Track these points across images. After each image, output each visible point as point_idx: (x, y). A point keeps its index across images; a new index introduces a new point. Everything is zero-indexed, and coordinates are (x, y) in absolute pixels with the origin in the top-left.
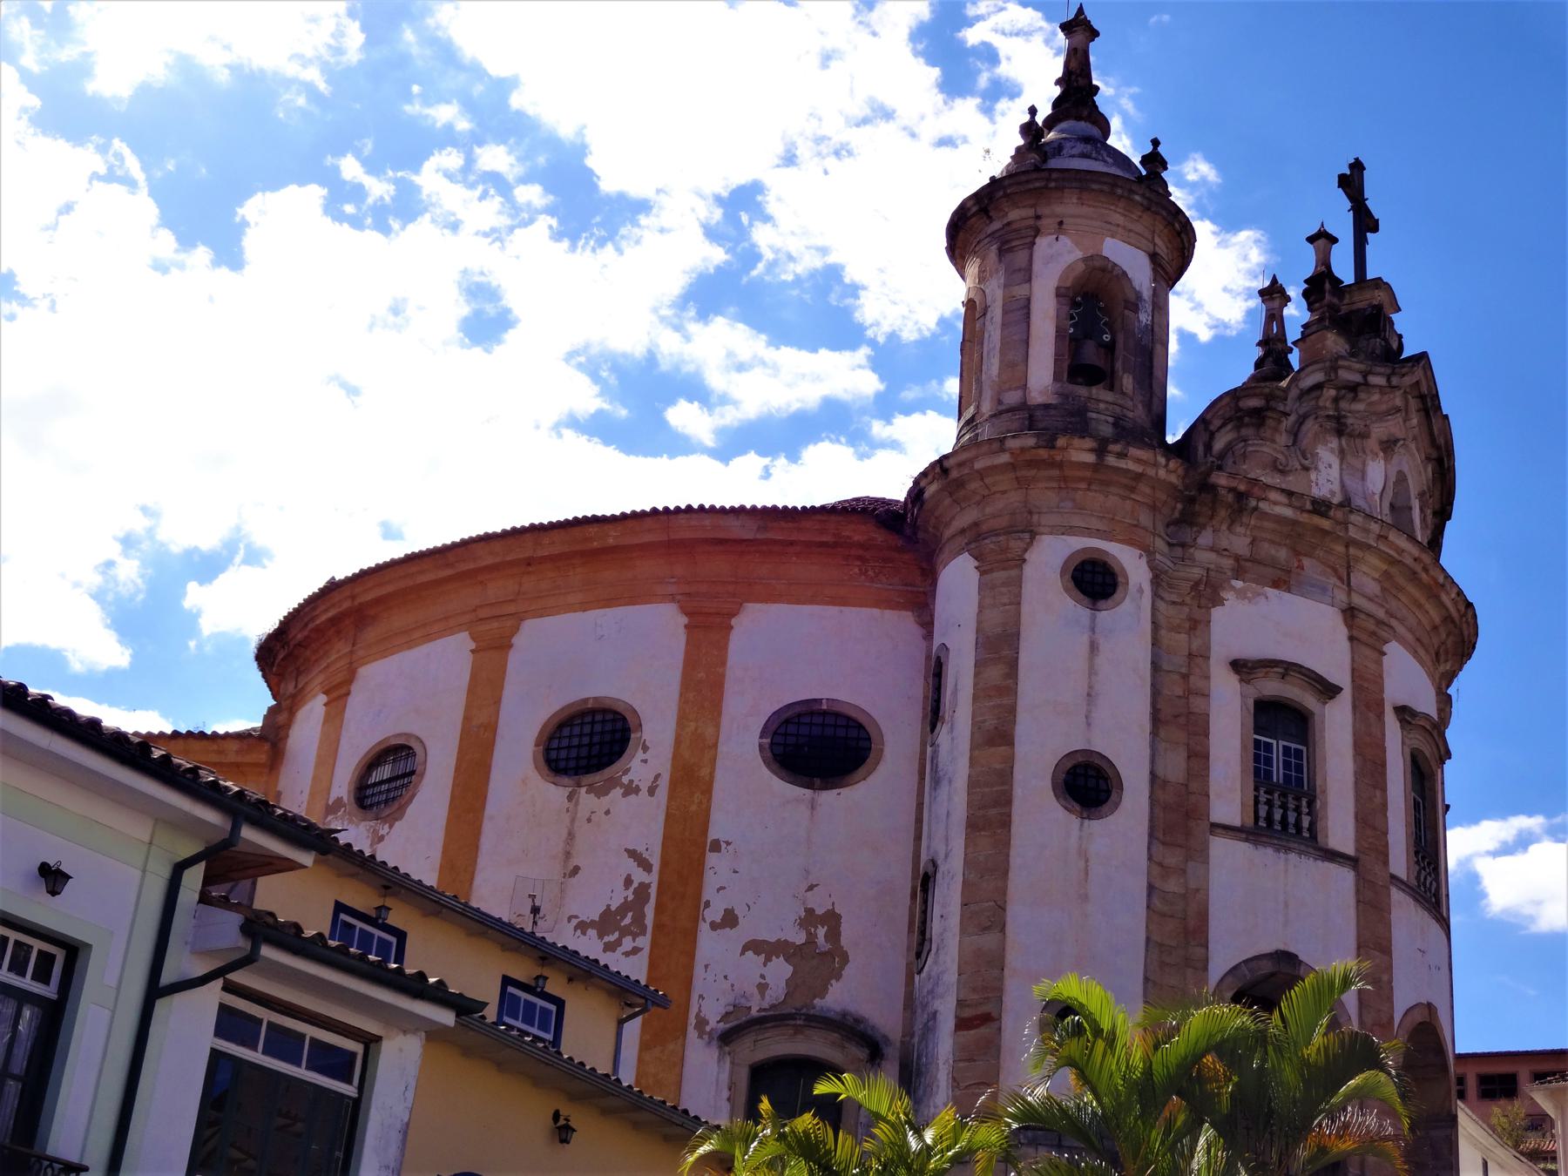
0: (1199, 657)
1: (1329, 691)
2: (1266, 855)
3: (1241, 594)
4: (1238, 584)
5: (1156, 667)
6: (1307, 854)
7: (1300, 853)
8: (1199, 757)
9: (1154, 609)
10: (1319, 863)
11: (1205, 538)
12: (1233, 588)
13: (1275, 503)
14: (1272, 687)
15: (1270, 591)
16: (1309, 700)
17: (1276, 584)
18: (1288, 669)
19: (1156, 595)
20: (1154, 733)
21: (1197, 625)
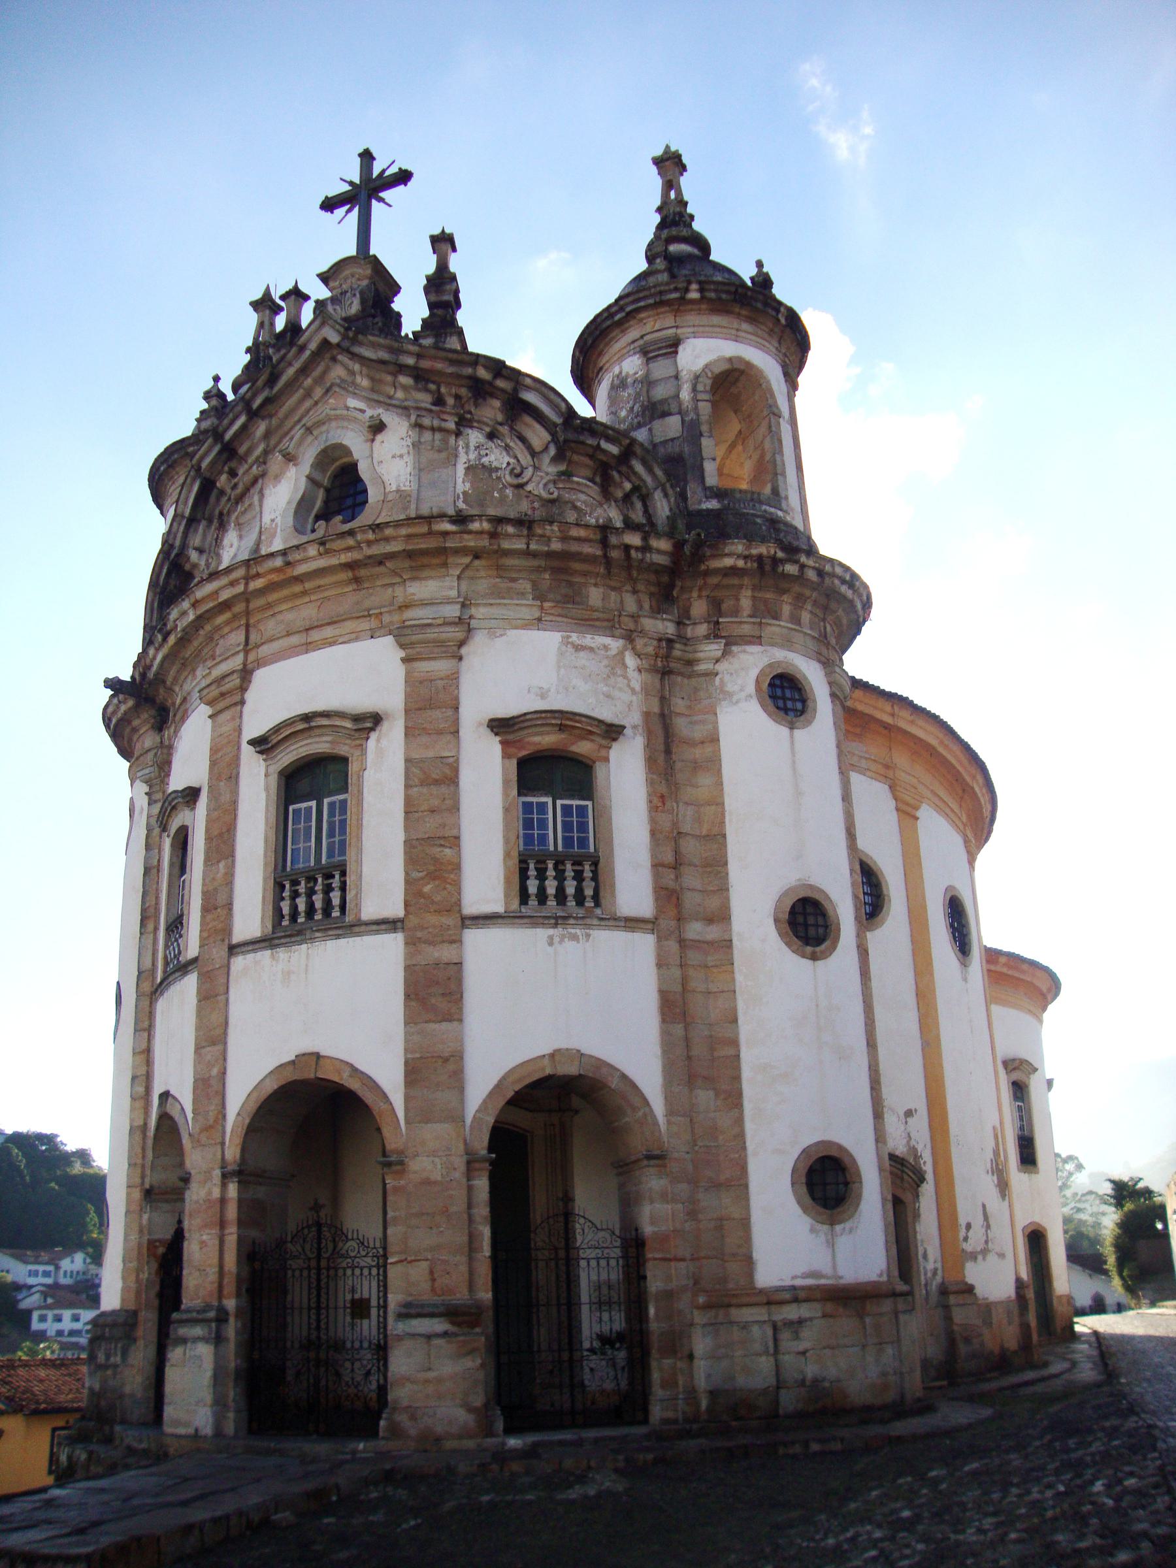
5: (147, 871)
13: (154, 658)
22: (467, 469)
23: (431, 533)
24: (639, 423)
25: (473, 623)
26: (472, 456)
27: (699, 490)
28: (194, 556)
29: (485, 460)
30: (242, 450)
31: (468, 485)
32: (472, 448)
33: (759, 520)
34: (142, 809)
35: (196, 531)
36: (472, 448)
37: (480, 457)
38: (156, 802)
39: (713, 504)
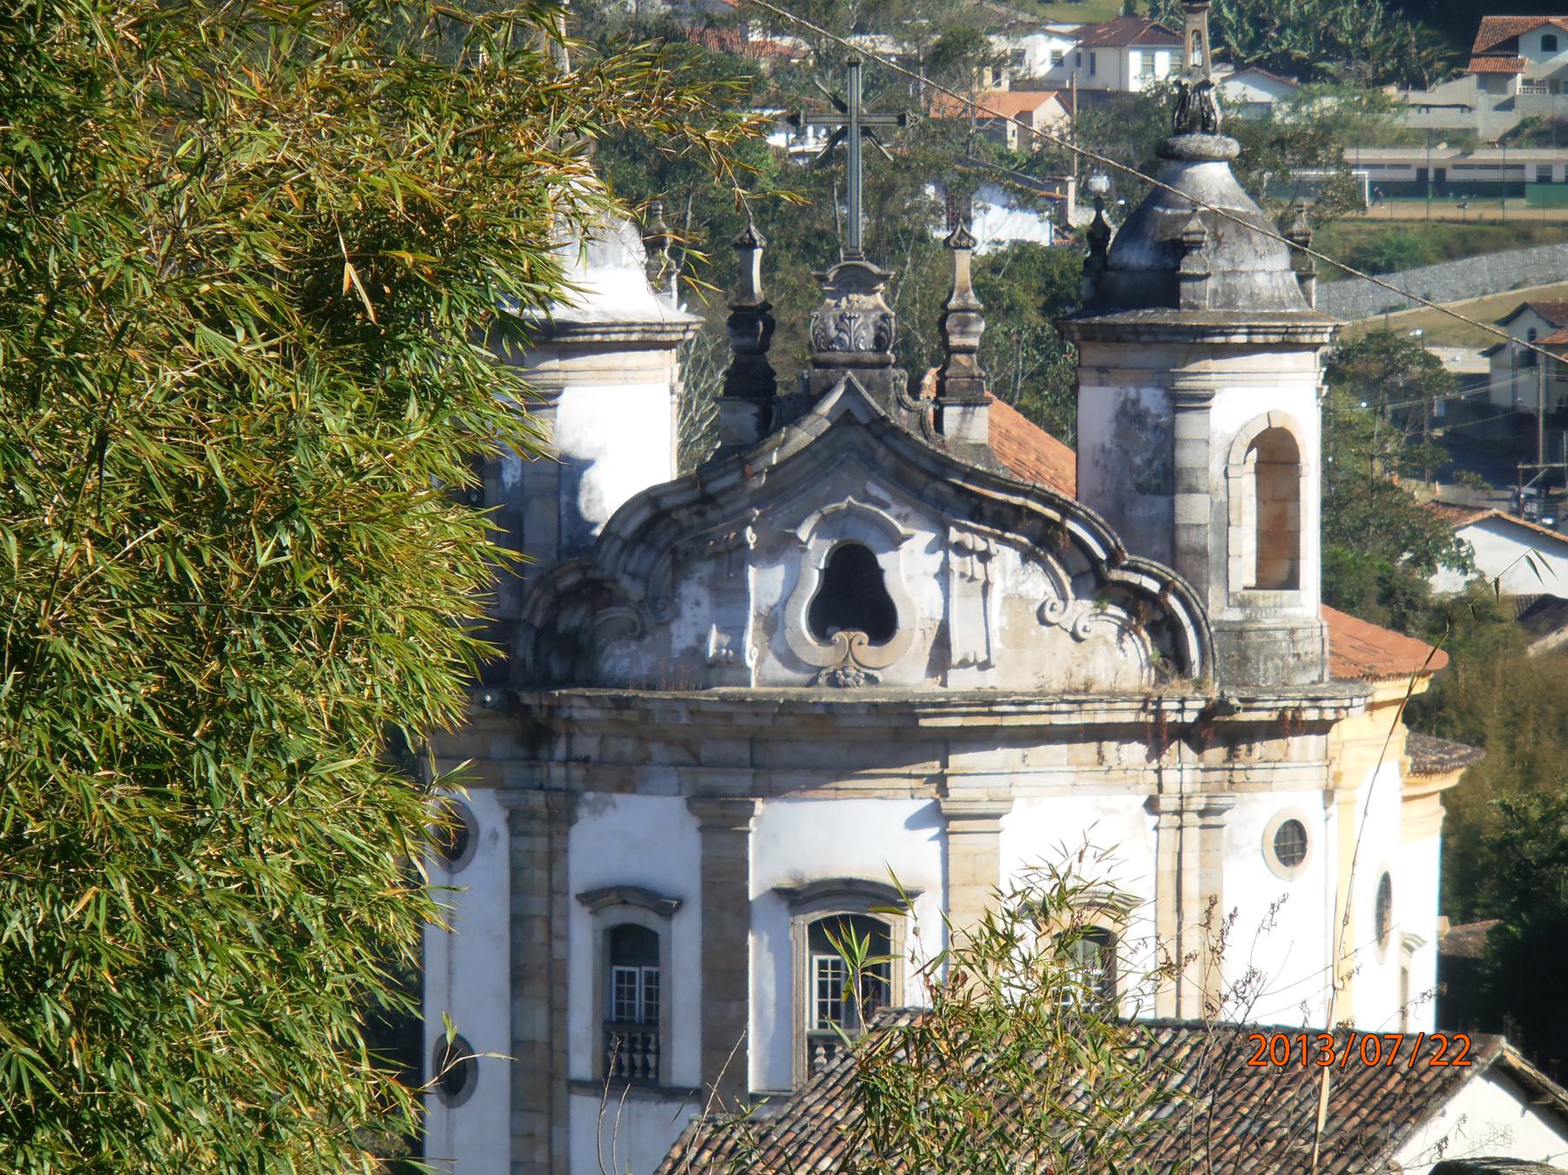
0: (556, 891)
1: (667, 906)
2: (618, 1110)
3: (597, 811)
4: (590, 796)
6: (648, 1100)
7: (642, 1100)
8: (558, 1009)
9: (513, 852)
10: (662, 1106)
11: (560, 751)
12: (587, 803)
14: (618, 915)
15: (617, 797)
16: (652, 921)
17: (621, 788)
18: (624, 893)
19: (514, 833)
20: (514, 996)
21: (556, 857)
22: (1005, 599)
23: (991, 714)
24: (1158, 486)
25: (1015, 791)
26: (1010, 583)
27: (1223, 594)
28: (625, 582)
29: (1022, 589)
30: (721, 500)
31: (1005, 619)
32: (1009, 572)
33: (1279, 635)
34: (495, 836)
35: (631, 555)
36: (1009, 572)
37: (1017, 584)
38: (524, 834)
39: (1235, 615)
